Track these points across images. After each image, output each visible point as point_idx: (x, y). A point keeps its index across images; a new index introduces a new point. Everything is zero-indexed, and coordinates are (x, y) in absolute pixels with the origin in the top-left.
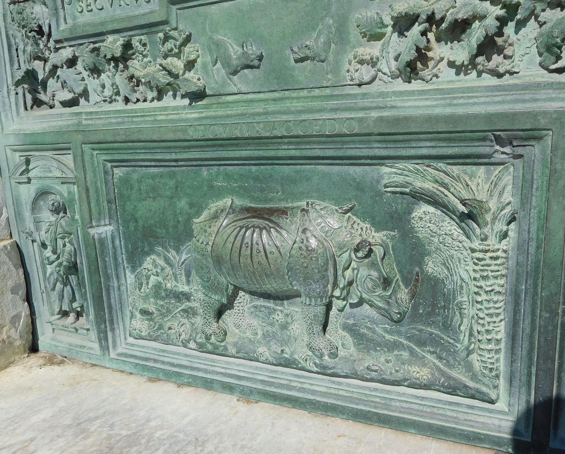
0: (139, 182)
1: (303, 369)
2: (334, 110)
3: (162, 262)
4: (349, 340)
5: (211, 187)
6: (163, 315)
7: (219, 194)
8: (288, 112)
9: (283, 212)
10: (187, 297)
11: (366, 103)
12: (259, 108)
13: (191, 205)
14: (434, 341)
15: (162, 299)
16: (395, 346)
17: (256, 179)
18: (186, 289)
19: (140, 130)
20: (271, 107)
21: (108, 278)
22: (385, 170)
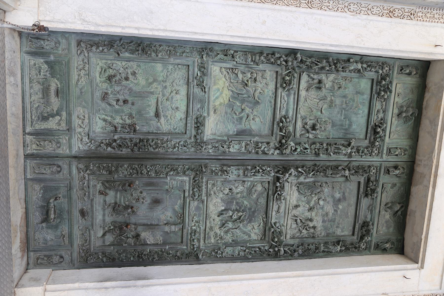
0: (62, 67)
1: (30, 99)
2: (73, 106)
3: (46, 69)
4: (37, 106)
5: (62, 83)
6: (35, 68)
7: (61, 84)
8: (73, 99)
9: (58, 97)
10: (40, 74)
11: (74, 111)
12: (74, 94)
13: (58, 78)
14: (39, 119)
15: (39, 68)
16: (37, 114)
17: (63, 91)
18: (42, 74)
19: (71, 71)
20: (74, 96)
21: (42, 56)
22: (65, 112)
